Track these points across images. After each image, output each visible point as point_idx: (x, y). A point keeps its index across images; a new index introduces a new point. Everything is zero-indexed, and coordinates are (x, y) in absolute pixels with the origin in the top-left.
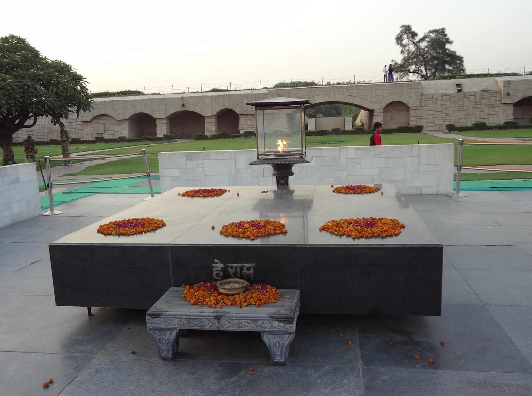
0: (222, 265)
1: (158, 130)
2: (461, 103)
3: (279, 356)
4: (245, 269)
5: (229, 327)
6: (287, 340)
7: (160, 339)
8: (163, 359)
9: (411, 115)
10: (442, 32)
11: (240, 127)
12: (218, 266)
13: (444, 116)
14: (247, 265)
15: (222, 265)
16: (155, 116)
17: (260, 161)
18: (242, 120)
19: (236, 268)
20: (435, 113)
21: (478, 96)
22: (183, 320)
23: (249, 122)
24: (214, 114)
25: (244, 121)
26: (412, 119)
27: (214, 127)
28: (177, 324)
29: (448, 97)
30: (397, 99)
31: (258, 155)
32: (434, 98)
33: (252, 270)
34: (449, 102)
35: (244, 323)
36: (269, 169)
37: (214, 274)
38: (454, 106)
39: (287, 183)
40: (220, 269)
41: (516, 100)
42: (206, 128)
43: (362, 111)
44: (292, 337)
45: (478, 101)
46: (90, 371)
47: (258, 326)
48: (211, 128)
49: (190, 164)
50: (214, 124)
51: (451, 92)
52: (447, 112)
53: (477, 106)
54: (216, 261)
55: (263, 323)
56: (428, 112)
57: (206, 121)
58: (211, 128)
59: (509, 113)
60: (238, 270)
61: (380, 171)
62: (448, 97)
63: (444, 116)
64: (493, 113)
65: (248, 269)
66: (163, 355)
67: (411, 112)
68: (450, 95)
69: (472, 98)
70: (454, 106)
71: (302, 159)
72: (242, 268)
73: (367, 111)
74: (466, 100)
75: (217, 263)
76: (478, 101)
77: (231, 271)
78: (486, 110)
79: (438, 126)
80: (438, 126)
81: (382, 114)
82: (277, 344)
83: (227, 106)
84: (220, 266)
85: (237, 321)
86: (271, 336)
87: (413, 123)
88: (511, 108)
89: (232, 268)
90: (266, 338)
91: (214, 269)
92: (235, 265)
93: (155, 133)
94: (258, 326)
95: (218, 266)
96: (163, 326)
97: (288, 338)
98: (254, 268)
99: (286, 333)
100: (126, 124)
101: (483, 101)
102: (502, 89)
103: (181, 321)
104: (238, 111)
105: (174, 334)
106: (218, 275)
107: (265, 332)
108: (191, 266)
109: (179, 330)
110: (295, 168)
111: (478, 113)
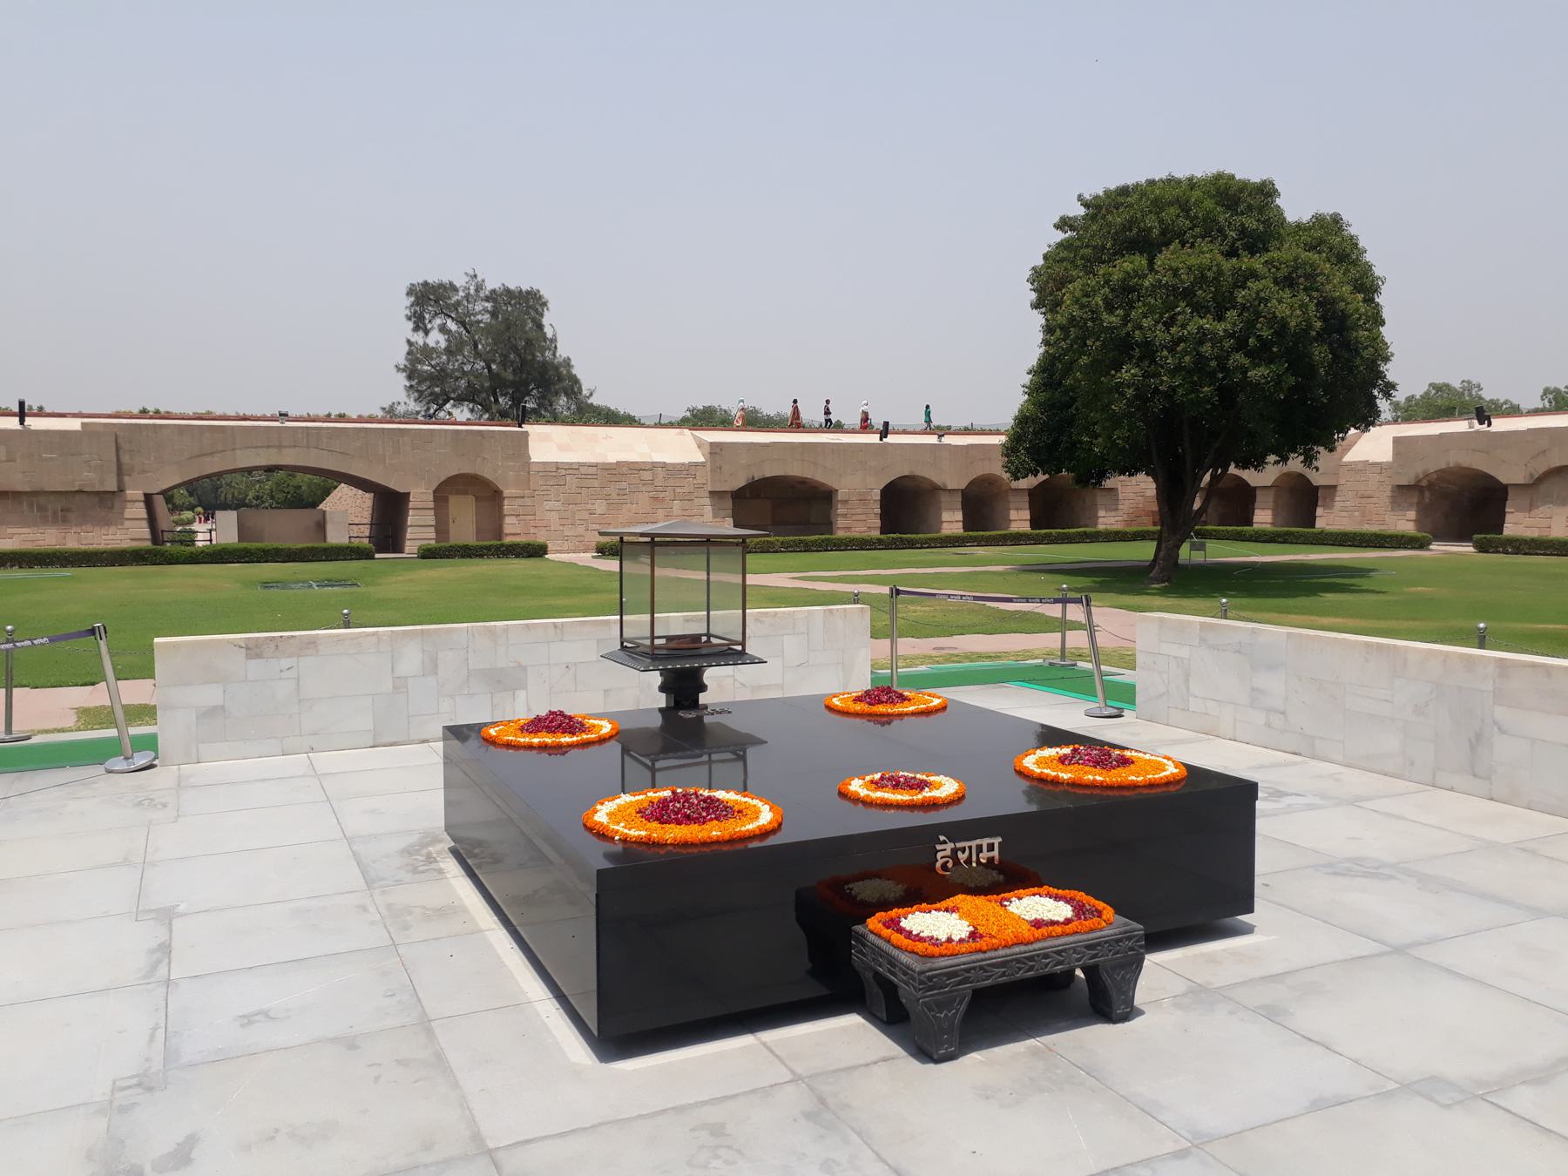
4: (985, 848)
10: (528, 304)
26: (508, 520)
30: (467, 469)
32: (557, 472)
37: (938, 865)
40: (948, 852)
43: (344, 490)
49: (254, 664)
54: (942, 838)
72: (979, 849)
73: (369, 496)
81: (432, 505)
84: (950, 846)
87: (514, 529)
88: (729, 503)
91: (939, 855)
95: (945, 850)
101: (671, 482)
106: (944, 866)
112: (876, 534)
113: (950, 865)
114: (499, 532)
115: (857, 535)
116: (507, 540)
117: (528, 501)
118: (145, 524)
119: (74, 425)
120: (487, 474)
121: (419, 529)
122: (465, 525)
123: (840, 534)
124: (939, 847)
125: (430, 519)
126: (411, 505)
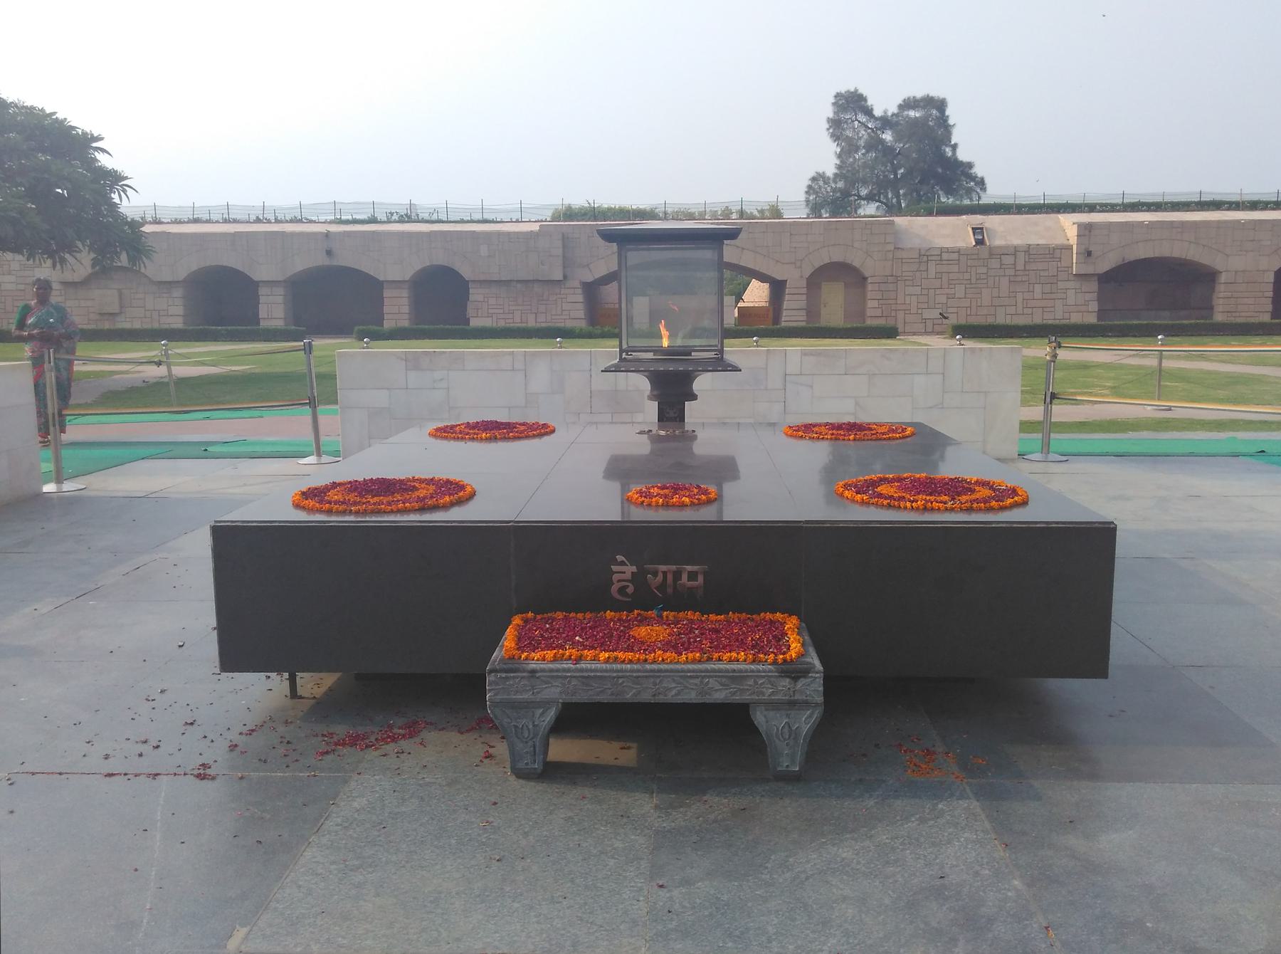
0: (634, 569)
1: (263, 313)
2: (984, 270)
3: (788, 758)
4: (685, 577)
5: (679, 693)
6: (805, 722)
7: (516, 727)
8: (520, 774)
9: (869, 295)
11: (470, 311)
12: (624, 571)
13: (943, 299)
14: (689, 568)
15: (634, 569)
16: (260, 273)
17: (625, 365)
18: (476, 294)
19: (665, 573)
20: (925, 292)
21: (1021, 257)
22: (574, 682)
23: (492, 301)
24: (407, 277)
25: (480, 298)
26: (870, 304)
27: (406, 309)
28: (554, 692)
29: (955, 256)
30: (837, 256)
31: (621, 351)
33: (701, 579)
34: (955, 268)
35: (713, 683)
36: (641, 383)
37: (614, 588)
38: (967, 276)
39: (681, 418)
40: (628, 576)
41: (1104, 266)
42: (386, 309)
43: (755, 284)
44: (817, 714)
45: (1020, 266)
46: (355, 804)
47: (742, 691)
48: (397, 309)
50: (406, 301)
51: (961, 244)
52: (952, 291)
53: (1019, 279)
54: (620, 558)
55: (756, 683)
56: (910, 290)
57: (387, 293)
58: (397, 309)
59: (1088, 297)
60: (670, 577)
61: (857, 404)
62: (955, 256)
63: (943, 299)
64: (1053, 296)
65: (693, 576)
66: (521, 765)
67: (870, 287)
68: (959, 251)
69: (1008, 260)
70: (967, 276)
71: (720, 364)
72: (677, 575)
73: (766, 286)
74: (994, 263)
75: (622, 563)
76: (1020, 266)
77: (655, 581)
78: (1038, 288)
79: (929, 324)
80: (929, 324)
81: (804, 291)
82: (786, 730)
83: (441, 259)
85: (697, 681)
86: (771, 714)
87: (874, 314)
88: (1094, 285)
89: (655, 574)
90: (760, 718)
91: (615, 577)
92: (663, 568)
93: (257, 321)
94: (742, 691)
95: (624, 571)
96: (526, 696)
97: (810, 716)
98: (705, 574)
99: (806, 704)
100: (178, 293)
101: (1033, 266)
102: (1073, 241)
103: (569, 682)
104: (466, 273)
105: (551, 714)
106: (622, 590)
107: (758, 703)
108: (559, 571)
109: (563, 704)
110: (702, 383)
111: (1020, 296)
112: (1266, 318)
113: (630, 590)
114: (862, 314)
115: (1239, 320)
116: (869, 322)
117: (891, 287)
118: (581, 306)
119: (536, 227)
120: (856, 264)
121: (793, 313)
122: (834, 306)
123: (1219, 317)
124: (614, 568)
125: (801, 302)
126: (787, 291)
